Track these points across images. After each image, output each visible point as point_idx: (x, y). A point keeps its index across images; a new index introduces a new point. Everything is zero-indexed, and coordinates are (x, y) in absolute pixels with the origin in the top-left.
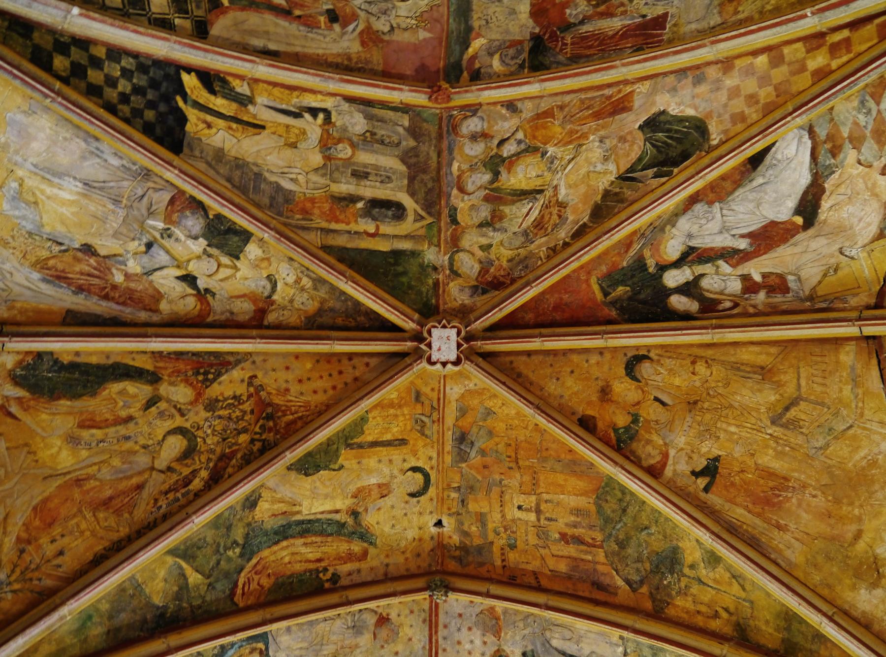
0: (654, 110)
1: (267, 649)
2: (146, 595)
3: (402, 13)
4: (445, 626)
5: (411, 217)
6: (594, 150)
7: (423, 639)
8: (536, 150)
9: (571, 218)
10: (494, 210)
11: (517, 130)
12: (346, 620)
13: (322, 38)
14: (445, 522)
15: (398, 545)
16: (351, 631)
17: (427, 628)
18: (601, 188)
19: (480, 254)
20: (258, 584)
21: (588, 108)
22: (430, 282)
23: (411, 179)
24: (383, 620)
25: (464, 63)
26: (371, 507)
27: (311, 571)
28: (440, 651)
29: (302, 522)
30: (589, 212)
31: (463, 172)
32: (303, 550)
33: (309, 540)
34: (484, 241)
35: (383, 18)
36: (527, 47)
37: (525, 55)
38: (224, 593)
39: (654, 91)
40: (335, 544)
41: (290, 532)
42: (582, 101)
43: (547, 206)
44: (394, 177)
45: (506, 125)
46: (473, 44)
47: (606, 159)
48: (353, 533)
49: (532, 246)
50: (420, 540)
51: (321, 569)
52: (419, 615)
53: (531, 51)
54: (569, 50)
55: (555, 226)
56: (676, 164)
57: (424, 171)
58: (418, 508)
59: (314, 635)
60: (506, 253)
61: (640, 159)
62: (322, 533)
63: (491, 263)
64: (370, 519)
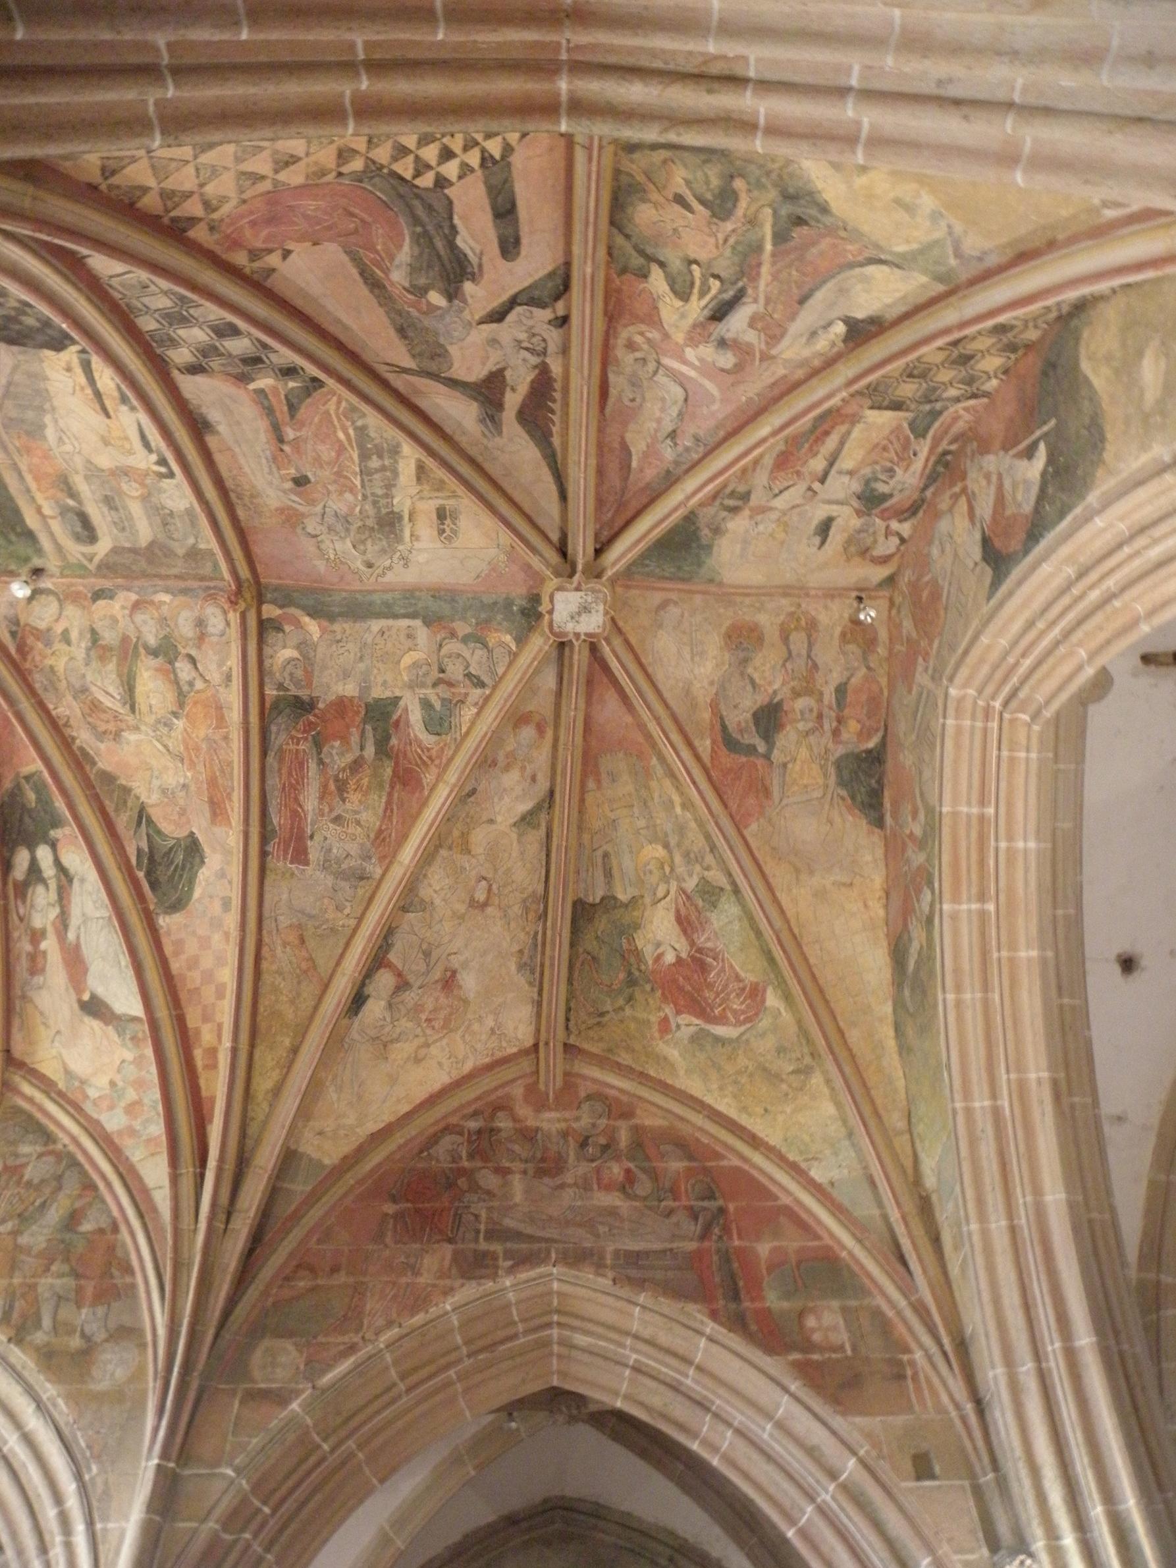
0: (207, 850)
3: (339, 546)
5: (88, 549)
6: (174, 776)
8: (181, 705)
9: (102, 746)
10: (111, 649)
11: (206, 681)
13: (266, 470)
18: (134, 785)
19: (59, 629)
21: (222, 771)
22: (13, 567)
23: (134, 551)
25: (292, 610)
30: (109, 769)
31: (158, 608)
34: (74, 635)
35: (324, 529)
36: (303, 694)
37: (294, 691)
39: (227, 852)
42: (230, 764)
43: (116, 717)
44: (127, 534)
45: (213, 667)
46: (313, 622)
47: (164, 791)
49: (69, 698)
53: (296, 697)
54: (291, 747)
55: (94, 728)
56: (148, 874)
57: (150, 562)
60: (60, 665)
61: (159, 832)
63: (48, 644)
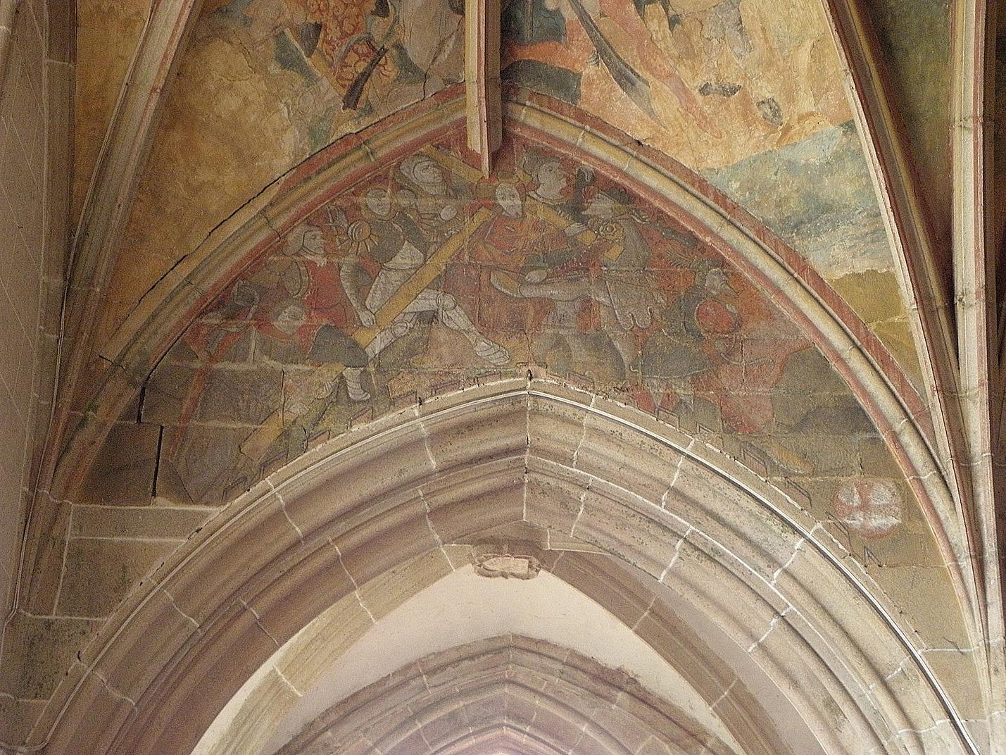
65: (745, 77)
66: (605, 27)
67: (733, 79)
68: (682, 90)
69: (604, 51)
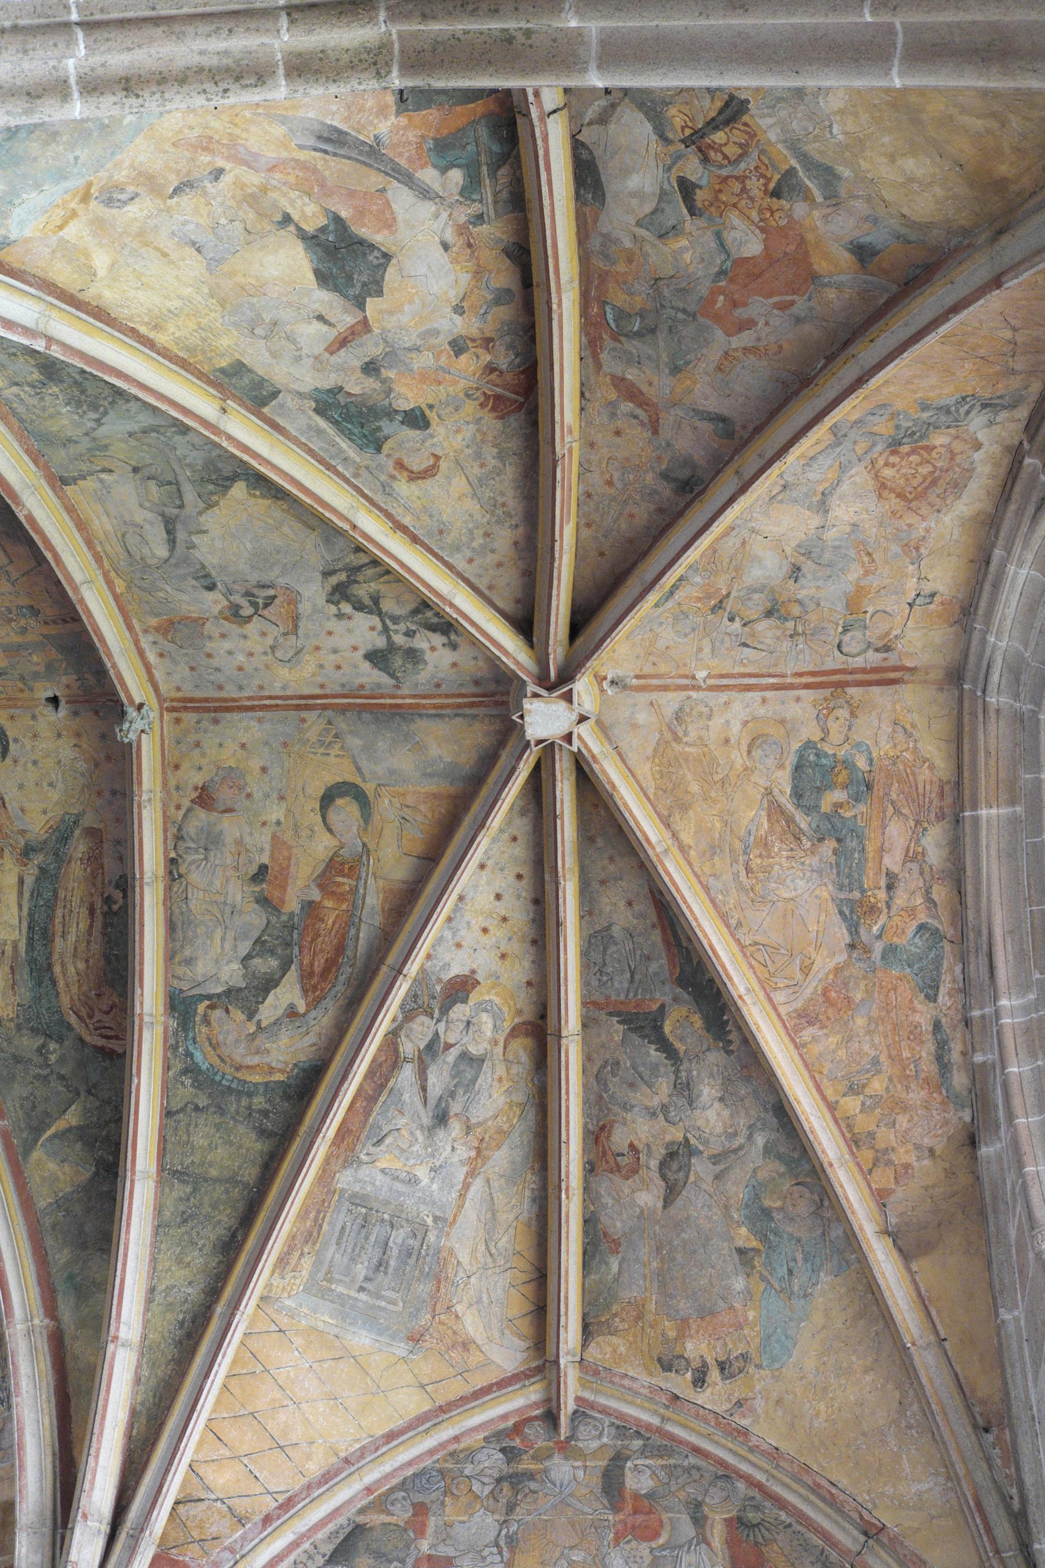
1: (209, 997)
2: (73, 1192)
4: (220, 688)
7: (245, 724)
12: (193, 862)
14: (50, 694)
15: (82, 774)
16: (212, 853)
17: (228, 715)
20: (108, 1013)
24: (204, 798)
26: (19, 825)
27: (105, 925)
28: (266, 693)
29: (30, 940)
32: (72, 938)
33: (59, 928)
38: (106, 1069)
40: (71, 885)
41: (42, 960)
48: (56, 854)
50: (78, 735)
51: (106, 908)
52: (205, 732)
58: (26, 741)
59: (208, 917)
62: (51, 907)
64: (37, 826)
65: (169, 210)
66: (374, 180)
67: (185, 201)
68: (249, 162)
69: (372, 154)
